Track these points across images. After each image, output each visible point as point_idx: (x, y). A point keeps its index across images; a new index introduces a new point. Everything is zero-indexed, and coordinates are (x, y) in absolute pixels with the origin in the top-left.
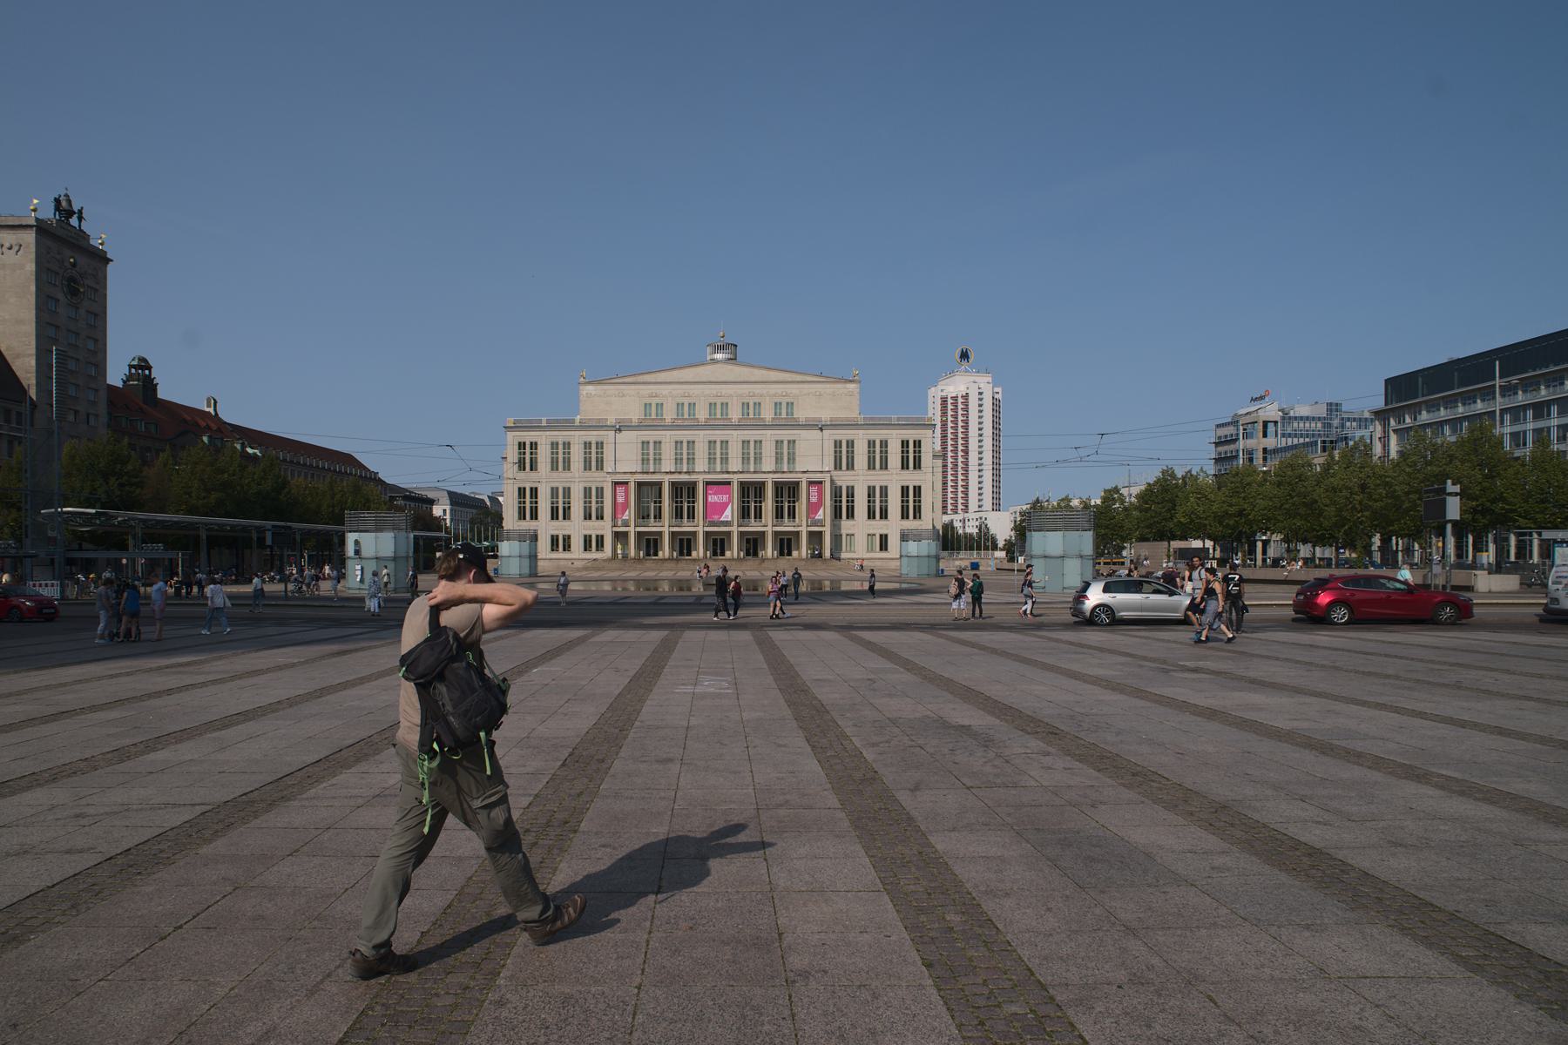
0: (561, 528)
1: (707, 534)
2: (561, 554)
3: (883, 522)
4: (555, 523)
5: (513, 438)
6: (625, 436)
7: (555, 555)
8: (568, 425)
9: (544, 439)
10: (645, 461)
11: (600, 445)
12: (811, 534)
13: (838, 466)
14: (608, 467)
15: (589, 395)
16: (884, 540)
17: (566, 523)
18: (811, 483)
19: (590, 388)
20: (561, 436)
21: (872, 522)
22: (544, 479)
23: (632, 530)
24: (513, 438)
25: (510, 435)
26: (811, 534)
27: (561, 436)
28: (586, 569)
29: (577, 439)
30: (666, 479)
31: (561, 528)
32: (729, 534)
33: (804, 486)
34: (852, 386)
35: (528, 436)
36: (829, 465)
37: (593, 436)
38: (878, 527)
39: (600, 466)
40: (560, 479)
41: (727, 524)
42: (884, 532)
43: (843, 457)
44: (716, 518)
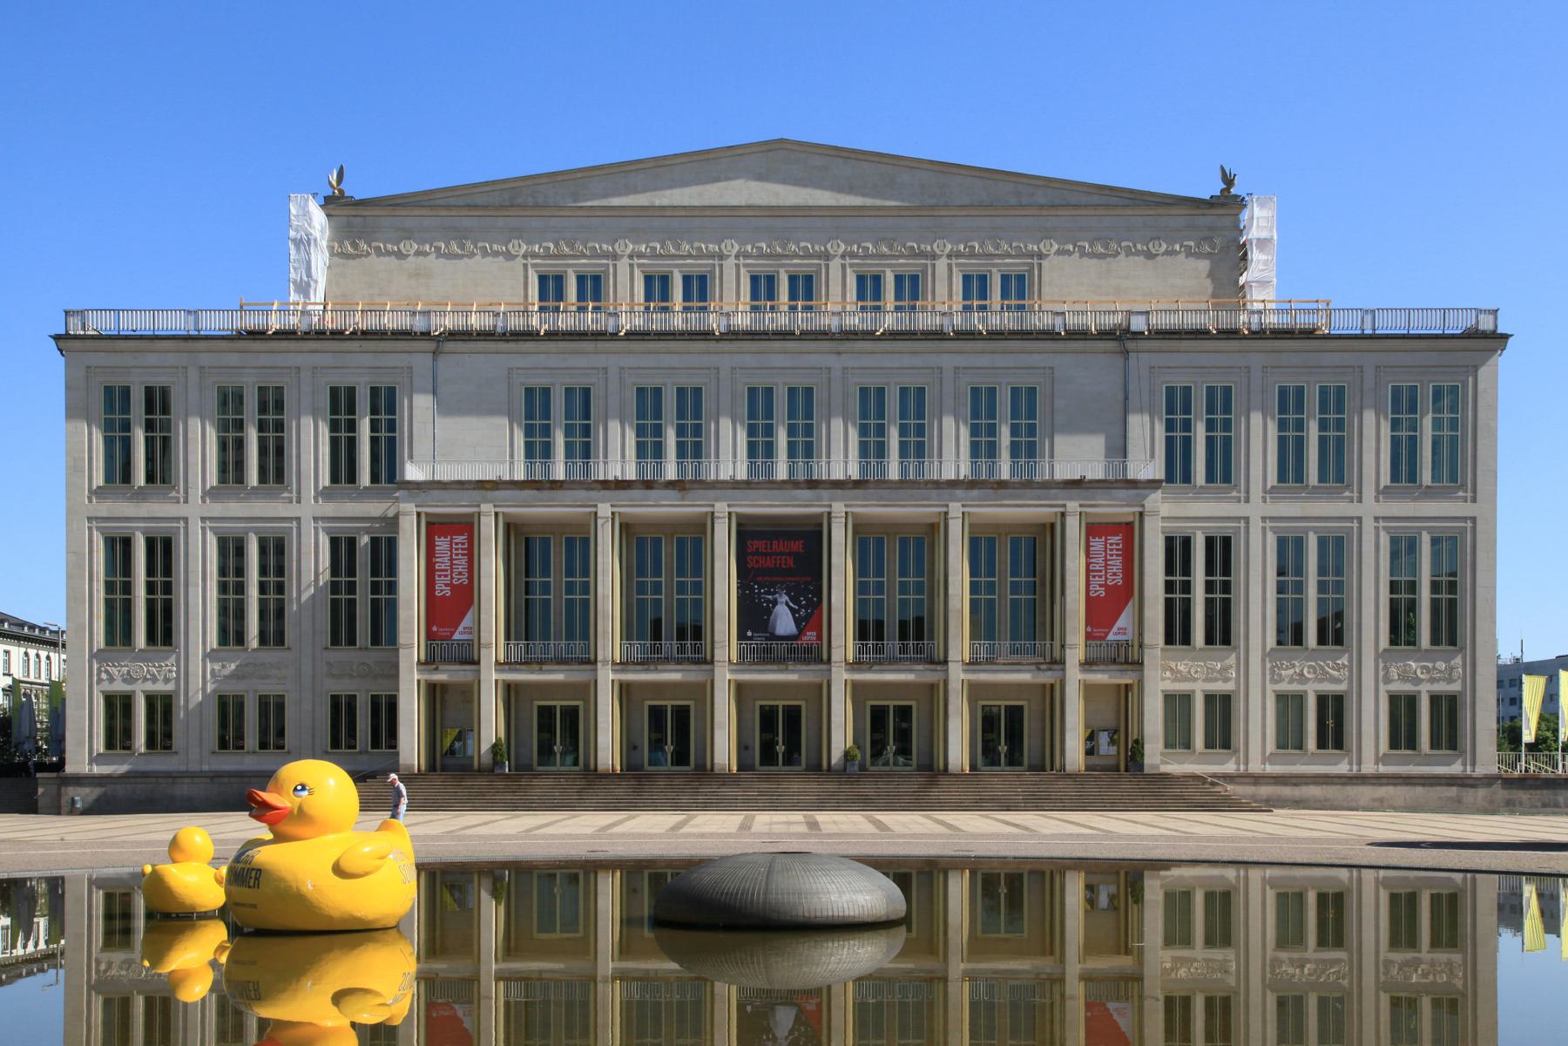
10: (538, 449)
13: (1177, 469)
26: (1089, 690)
36: (1146, 464)
38: (1312, 675)
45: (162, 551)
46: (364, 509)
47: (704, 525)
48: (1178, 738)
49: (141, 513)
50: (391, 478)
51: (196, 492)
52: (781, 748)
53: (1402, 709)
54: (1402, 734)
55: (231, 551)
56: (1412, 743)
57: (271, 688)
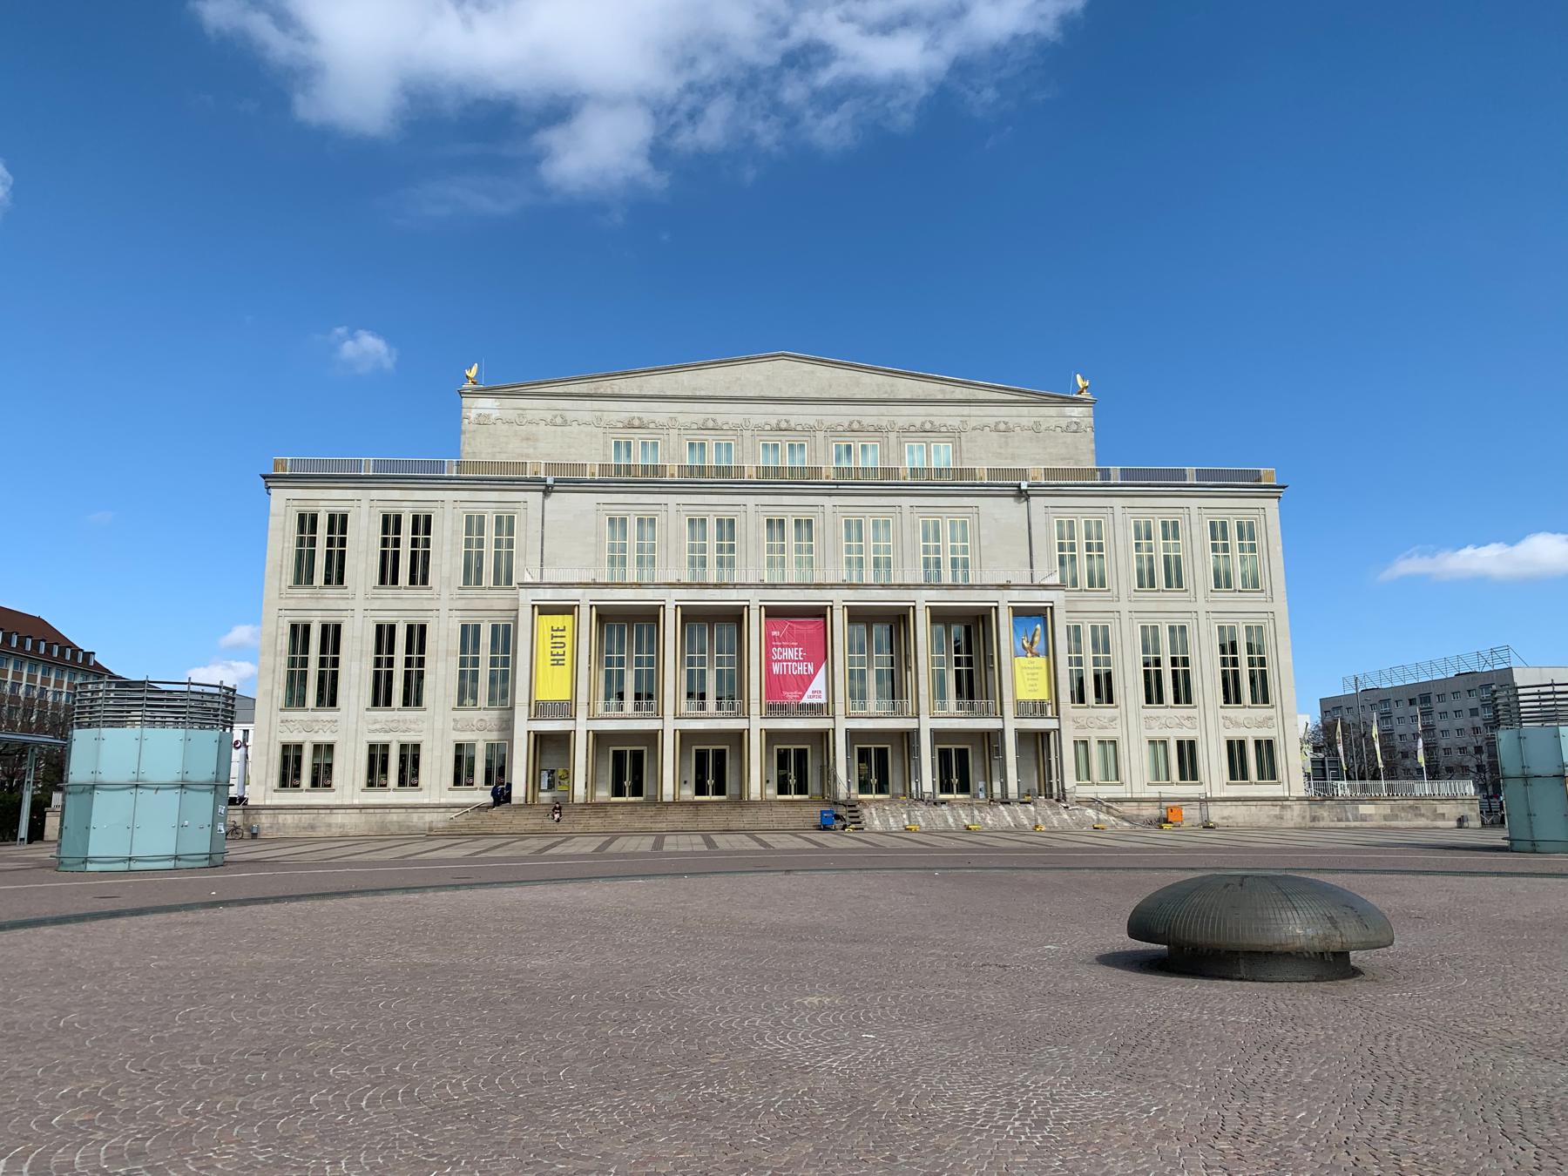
0: (396, 727)
1: (771, 736)
2: (392, 795)
3: (1182, 711)
4: (382, 714)
5: (284, 505)
6: (561, 502)
7: (376, 797)
8: (430, 476)
9: (365, 513)
10: (618, 561)
11: (505, 525)
12: (1022, 735)
14: (525, 571)
15: (482, 421)
16: (1188, 754)
17: (411, 714)
18: (1018, 612)
19: (486, 405)
20: (407, 502)
21: (1155, 711)
22: (360, 606)
23: (582, 728)
24: (284, 505)
25: (279, 496)
26: (1022, 735)
27: (407, 502)
28: (452, 834)
29: (450, 512)
30: (671, 601)
31: (396, 727)
32: (822, 737)
33: (1005, 618)
34: (1075, 412)
35: (325, 501)
37: (489, 503)
38: (1172, 723)
39: (504, 576)
40: (401, 605)
41: (815, 710)
42: (1186, 734)
43: (1082, 564)
44: (791, 696)
45: (332, 636)
46: (489, 604)
47: (742, 616)
48: (1084, 772)
49: (318, 606)
50: (509, 581)
51: (360, 594)
52: (792, 781)
53: (1235, 750)
54: (1237, 770)
55: (385, 635)
56: (1245, 776)
57: (409, 738)
